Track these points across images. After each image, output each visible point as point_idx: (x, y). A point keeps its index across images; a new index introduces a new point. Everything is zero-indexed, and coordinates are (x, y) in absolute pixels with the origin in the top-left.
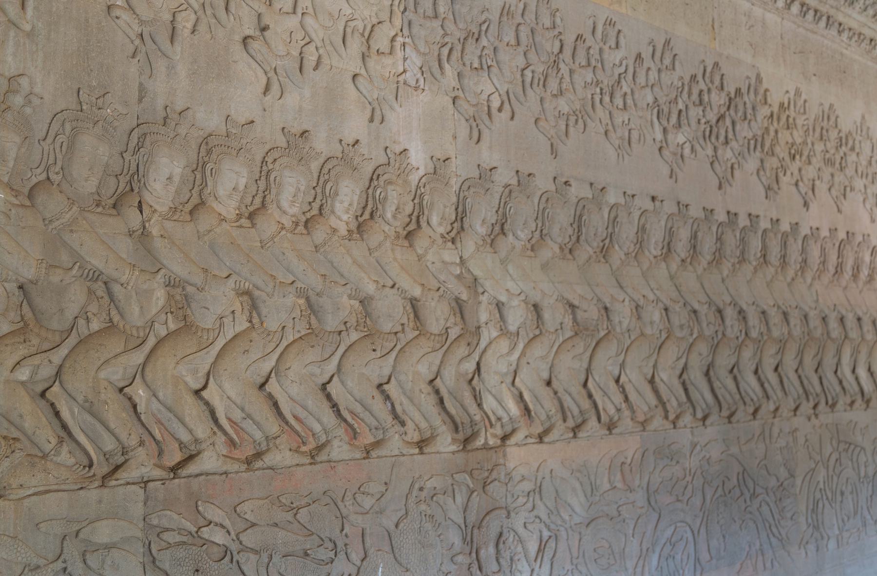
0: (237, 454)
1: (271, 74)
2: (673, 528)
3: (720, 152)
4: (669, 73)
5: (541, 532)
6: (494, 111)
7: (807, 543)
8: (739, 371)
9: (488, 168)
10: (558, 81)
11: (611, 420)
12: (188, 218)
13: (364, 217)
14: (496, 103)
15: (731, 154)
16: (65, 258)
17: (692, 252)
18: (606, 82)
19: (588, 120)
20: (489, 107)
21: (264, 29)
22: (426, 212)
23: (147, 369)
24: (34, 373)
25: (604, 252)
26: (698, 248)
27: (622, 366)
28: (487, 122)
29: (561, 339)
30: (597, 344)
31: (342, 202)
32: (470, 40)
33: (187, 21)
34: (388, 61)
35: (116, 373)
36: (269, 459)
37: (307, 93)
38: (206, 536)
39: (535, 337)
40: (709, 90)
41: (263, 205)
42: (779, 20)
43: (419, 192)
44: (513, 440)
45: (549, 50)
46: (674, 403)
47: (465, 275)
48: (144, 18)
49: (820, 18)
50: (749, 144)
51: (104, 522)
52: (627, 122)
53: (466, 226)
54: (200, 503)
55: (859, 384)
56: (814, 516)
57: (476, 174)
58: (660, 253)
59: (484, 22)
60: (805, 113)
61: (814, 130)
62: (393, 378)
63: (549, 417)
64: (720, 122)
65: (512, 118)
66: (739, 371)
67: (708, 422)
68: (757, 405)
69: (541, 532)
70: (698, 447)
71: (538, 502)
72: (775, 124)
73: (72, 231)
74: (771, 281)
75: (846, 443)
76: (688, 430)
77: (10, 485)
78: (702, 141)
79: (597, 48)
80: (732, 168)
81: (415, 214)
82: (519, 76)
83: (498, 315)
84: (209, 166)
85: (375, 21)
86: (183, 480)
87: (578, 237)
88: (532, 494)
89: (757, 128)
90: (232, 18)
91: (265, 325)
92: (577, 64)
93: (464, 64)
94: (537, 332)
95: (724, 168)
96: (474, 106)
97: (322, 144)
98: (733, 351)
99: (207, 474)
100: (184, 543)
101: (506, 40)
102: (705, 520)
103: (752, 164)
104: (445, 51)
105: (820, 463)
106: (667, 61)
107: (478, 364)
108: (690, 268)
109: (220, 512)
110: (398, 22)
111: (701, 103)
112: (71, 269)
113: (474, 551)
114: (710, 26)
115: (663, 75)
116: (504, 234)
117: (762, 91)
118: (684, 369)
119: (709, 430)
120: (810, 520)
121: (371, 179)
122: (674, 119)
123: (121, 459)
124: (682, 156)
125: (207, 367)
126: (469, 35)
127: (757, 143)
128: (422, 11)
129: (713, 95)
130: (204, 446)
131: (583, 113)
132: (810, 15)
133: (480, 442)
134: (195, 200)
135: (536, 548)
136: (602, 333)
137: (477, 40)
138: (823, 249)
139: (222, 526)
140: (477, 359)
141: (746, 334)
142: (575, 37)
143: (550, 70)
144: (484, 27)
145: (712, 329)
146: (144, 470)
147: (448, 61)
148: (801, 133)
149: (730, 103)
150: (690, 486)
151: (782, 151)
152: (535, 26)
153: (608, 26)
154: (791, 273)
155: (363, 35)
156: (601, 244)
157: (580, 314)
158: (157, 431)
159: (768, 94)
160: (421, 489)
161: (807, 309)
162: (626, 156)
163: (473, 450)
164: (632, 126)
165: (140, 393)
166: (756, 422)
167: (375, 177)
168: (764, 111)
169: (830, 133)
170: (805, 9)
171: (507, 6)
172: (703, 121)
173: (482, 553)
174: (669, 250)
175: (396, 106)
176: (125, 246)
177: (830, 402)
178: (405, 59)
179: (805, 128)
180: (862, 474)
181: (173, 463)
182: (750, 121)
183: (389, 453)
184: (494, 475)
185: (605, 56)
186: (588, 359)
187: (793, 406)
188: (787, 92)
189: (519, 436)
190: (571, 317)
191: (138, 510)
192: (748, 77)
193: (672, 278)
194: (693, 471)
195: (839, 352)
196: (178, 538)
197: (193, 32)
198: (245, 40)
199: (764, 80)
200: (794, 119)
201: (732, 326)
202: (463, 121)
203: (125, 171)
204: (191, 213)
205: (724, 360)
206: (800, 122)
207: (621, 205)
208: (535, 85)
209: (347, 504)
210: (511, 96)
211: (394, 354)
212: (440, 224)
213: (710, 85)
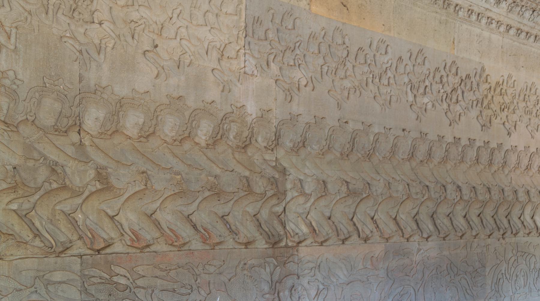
0: (136, 244)
1: (160, 69)
2: (402, 287)
3: (451, 107)
4: (420, 67)
5: (318, 286)
6: (302, 87)
7: (490, 298)
8: (453, 216)
9: (296, 115)
10: (344, 71)
11: (367, 236)
13: (217, 138)
14: (303, 82)
15: (460, 108)
16: (36, 155)
17: (428, 157)
18: (377, 72)
19: (363, 91)
20: (299, 84)
21: (156, 46)
22: (255, 136)
23: (83, 206)
25: (369, 156)
26: (432, 155)
27: (376, 211)
28: (297, 92)
29: (338, 198)
30: (361, 201)
31: (201, 131)
32: (288, 51)
33: (110, 44)
34: (234, 62)
35: (67, 207)
36: (153, 248)
37: (183, 78)
38: (115, 280)
39: (322, 196)
40: (448, 76)
42: (501, 38)
43: (252, 126)
44: (303, 244)
45: (340, 55)
46: (409, 229)
47: (278, 166)
48: (82, 42)
49: (530, 37)
50: (472, 103)
51: (58, 272)
52: (389, 92)
53: (280, 143)
54: (112, 266)
55: (535, 224)
56: (496, 286)
57: (289, 117)
58: (406, 157)
59: (298, 42)
60: (514, 87)
61: (519, 96)
62: (231, 214)
63: (328, 234)
64: (453, 92)
65: (313, 90)
66: (453, 216)
67: (429, 240)
68: (464, 232)
69: (318, 286)
70: (422, 251)
71: (317, 273)
72: (492, 93)
73: (39, 143)
74: (480, 172)
75: (522, 252)
76: (416, 243)
77: (6, 254)
78: (440, 102)
79: (372, 54)
80: (460, 115)
81: (249, 136)
82: (319, 69)
83: (300, 186)
85: (227, 42)
86: (102, 256)
87: (352, 149)
88: (314, 269)
89: (479, 95)
90: (135, 41)
92: (358, 62)
93: (284, 64)
94: (324, 194)
95: (454, 115)
96: (289, 84)
97: (191, 102)
98: (450, 206)
99: (117, 253)
100: (103, 283)
101: (311, 50)
102: (423, 284)
103: (474, 113)
104: (272, 57)
105: (504, 261)
106: (419, 60)
107: (285, 208)
108: (426, 165)
109: (124, 270)
110: (242, 43)
111: (441, 82)
112: (39, 160)
113: (277, 293)
114: (452, 42)
115: (416, 68)
116: (304, 147)
117: (485, 76)
118: (417, 213)
119: (430, 243)
120: (493, 288)
121: (222, 120)
122: (421, 90)
123: (69, 245)
124: (426, 110)
126: (288, 48)
127: (479, 102)
128: (257, 37)
129: (450, 78)
130: (115, 241)
131: (360, 87)
132: (523, 35)
133: (283, 244)
135: (315, 293)
136: (364, 196)
137: (293, 51)
138: (519, 157)
139: (126, 277)
140: (284, 206)
141: (461, 197)
142: (357, 49)
143: (339, 66)
144: (298, 44)
145: (437, 195)
147: (273, 62)
148: (510, 97)
149: (461, 82)
150: (415, 269)
151: (495, 107)
152: (331, 44)
153: (380, 43)
154: (494, 168)
155: (219, 49)
156: (368, 153)
157: (351, 186)
158: (89, 233)
159: (489, 77)
160: (245, 264)
161: (504, 186)
162: (387, 109)
163: (278, 248)
164: (392, 93)
165: (79, 216)
166: (462, 241)
167: (224, 119)
168: (484, 87)
169: (530, 97)
170: (519, 32)
171: (313, 34)
172: (442, 91)
173: (281, 294)
174: (412, 156)
175: (239, 85)
176: (70, 150)
177: (514, 232)
178: (245, 61)
179: (513, 95)
180: (532, 267)
182: (474, 91)
183: (226, 247)
184: (290, 259)
185: (377, 58)
186: (355, 208)
187: (489, 233)
188: (502, 76)
189: (308, 242)
190: (346, 187)
192: (475, 69)
193: (412, 169)
194: (417, 262)
195: (523, 209)
196: (99, 281)
197: (113, 49)
198: (144, 53)
199: (486, 70)
200: (506, 90)
201: (451, 194)
202: (281, 91)
203: (73, 115)
205: (444, 210)
206: (510, 91)
207: (382, 133)
208: (329, 74)
209: (199, 269)
210: (313, 79)
211: (232, 202)
212: (263, 142)
213: (448, 73)
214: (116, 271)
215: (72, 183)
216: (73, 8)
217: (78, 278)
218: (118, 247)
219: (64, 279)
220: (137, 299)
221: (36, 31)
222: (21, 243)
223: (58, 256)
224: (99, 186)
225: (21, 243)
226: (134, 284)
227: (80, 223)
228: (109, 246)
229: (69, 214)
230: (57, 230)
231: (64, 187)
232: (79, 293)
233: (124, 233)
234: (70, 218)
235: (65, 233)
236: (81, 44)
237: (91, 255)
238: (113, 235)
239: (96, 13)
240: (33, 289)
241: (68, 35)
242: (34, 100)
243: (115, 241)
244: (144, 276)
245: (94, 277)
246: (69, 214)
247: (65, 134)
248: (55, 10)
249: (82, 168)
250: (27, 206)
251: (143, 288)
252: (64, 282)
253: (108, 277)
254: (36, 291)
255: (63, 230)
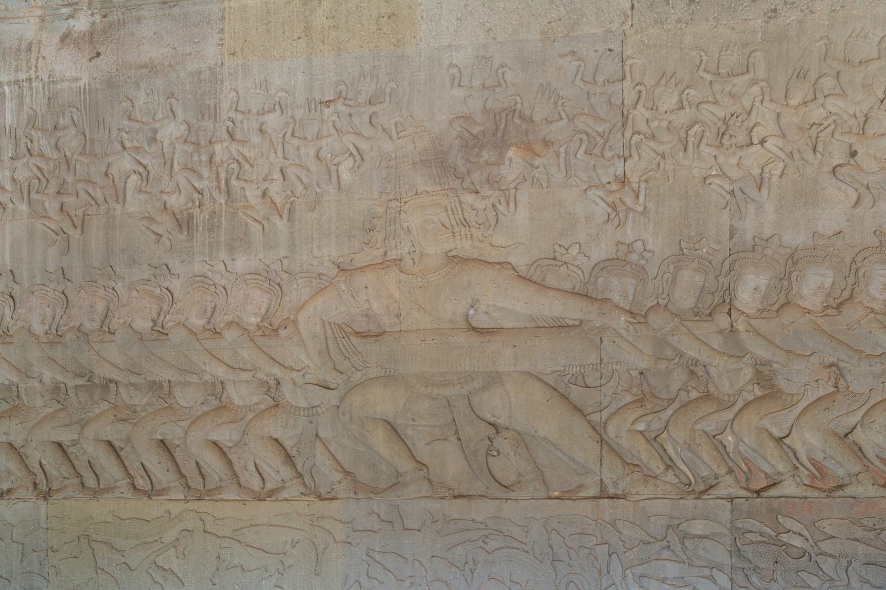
12: (774, 315)
16: (669, 353)
23: (735, 423)
24: (648, 425)
35: (710, 425)
36: (849, 491)
38: (785, 540)
41: (852, 297)
54: (779, 516)
84: (794, 275)
91: (850, 389)
100: (765, 542)
109: (799, 524)
123: (714, 482)
125: (791, 422)
130: (784, 477)
134: (782, 300)
139: (802, 536)
146: (730, 490)
165: (729, 439)
176: (716, 342)
181: (759, 488)
191: (726, 516)
196: (759, 538)
204: (777, 311)
214: (785, 525)
215: (717, 389)
216: (721, 131)
217: (727, 532)
218: (789, 488)
219: (707, 533)
220: (821, 573)
221: (671, 179)
222: (649, 477)
223: (699, 498)
224: (758, 392)
225: (649, 477)
226: (816, 548)
227: (730, 449)
228: (774, 484)
229: (714, 437)
230: (696, 460)
231: (707, 397)
232: (729, 555)
233: (799, 465)
234: (715, 442)
235: (708, 463)
236: (732, 181)
237: (747, 499)
238: (781, 468)
239: (755, 130)
240: (664, 543)
241: (714, 173)
242: (667, 276)
243: (784, 477)
244: (833, 537)
245: (751, 532)
246: (714, 437)
247: (710, 318)
248: (697, 143)
249: (733, 367)
250: (657, 425)
251: (831, 556)
252: (706, 537)
253: (773, 534)
254: (669, 547)
255: (706, 460)
